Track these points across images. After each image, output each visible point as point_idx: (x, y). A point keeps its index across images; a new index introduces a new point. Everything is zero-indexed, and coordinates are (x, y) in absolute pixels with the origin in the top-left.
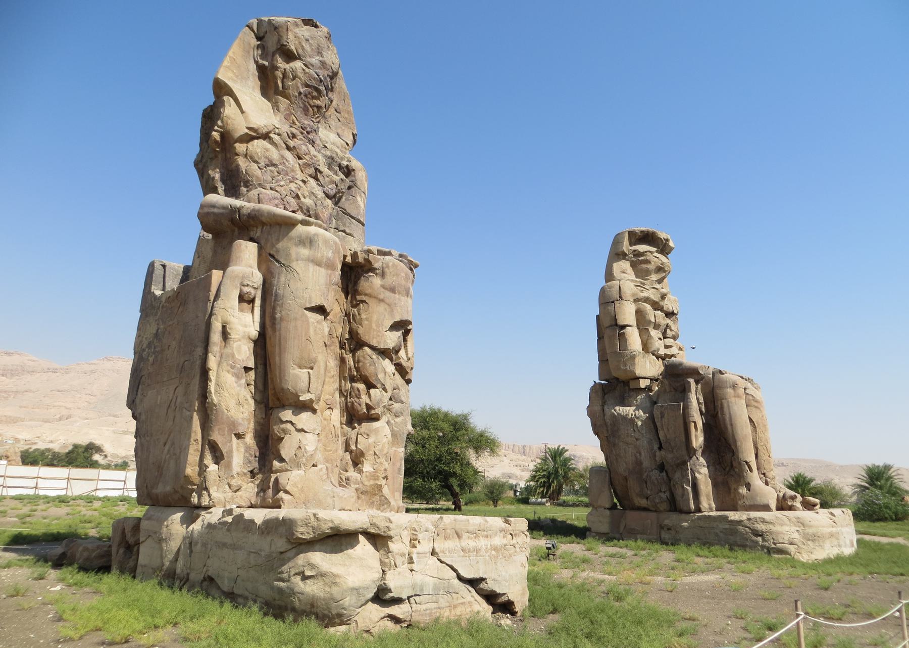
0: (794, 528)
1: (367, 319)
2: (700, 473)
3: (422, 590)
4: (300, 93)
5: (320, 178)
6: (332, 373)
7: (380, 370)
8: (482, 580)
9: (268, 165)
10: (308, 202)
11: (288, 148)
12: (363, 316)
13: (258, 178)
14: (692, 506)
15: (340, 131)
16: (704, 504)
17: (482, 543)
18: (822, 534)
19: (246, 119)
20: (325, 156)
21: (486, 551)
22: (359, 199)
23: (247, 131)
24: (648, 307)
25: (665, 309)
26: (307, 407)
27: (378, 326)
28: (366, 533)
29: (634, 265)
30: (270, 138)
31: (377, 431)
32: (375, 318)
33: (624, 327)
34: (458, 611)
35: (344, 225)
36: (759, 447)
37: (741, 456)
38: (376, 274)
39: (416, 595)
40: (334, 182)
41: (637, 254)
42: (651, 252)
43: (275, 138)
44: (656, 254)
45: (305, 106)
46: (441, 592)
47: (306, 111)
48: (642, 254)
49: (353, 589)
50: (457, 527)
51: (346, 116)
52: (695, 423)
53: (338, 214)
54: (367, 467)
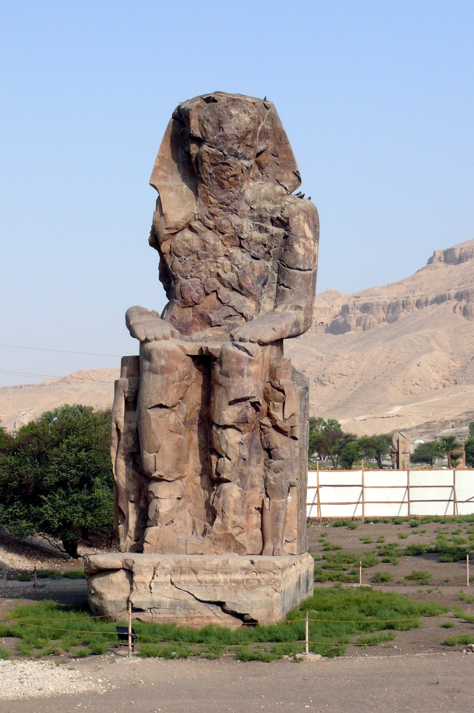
1: (213, 401)
4: (210, 174)
5: (245, 245)
7: (223, 442)
8: (224, 603)
9: (188, 255)
10: (228, 276)
11: (210, 229)
12: (212, 399)
13: (181, 272)
15: (278, 176)
19: (165, 219)
20: (252, 218)
21: (226, 582)
22: (296, 246)
23: (166, 232)
26: (160, 479)
28: (124, 569)
30: (191, 228)
31: (225, 492)
32: (217, 399)
34: (196, 621)
35: (284, 278)
38: (217, 362)
39: (154, 608)
43: (196, 224)
45: (219, 182)
46: (178, 607)
47: (221, 186)
49: (111, 601)
50: (193, 566)
51: (284, 156)
53: (279, 267)
54: (218, 521)
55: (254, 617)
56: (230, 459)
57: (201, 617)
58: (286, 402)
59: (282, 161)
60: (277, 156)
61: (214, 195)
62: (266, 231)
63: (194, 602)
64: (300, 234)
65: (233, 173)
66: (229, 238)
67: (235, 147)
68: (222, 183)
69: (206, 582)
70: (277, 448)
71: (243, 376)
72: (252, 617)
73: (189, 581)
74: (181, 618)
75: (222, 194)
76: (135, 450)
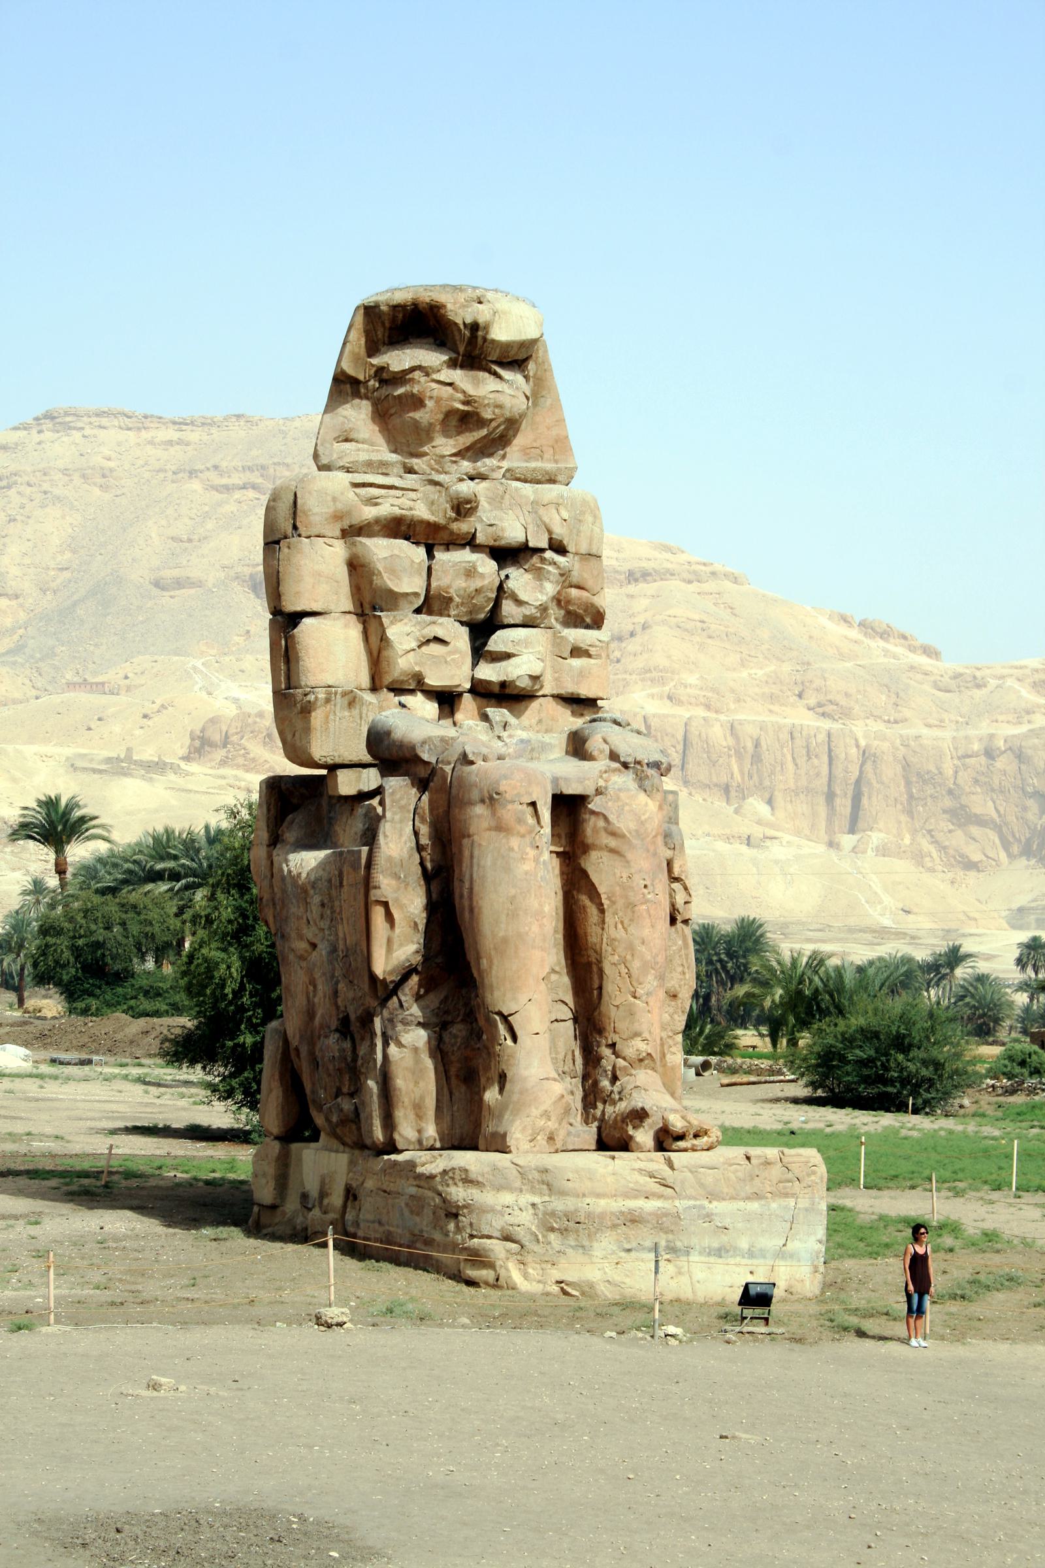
0: (527, 1198)
2: (400, 1045)
14: (379, 1134)
16: (406, 1131)
18: (589, 1215)
24: (382, 550)
25: (480, 539)
29: (382, 415)
33: (295, 618)
36: (608, 969)
37: (489, 999)
41: (387, 379)
42: (426, 371)
44: (447, 375)
48: (401, 378)
52: (386, 905)
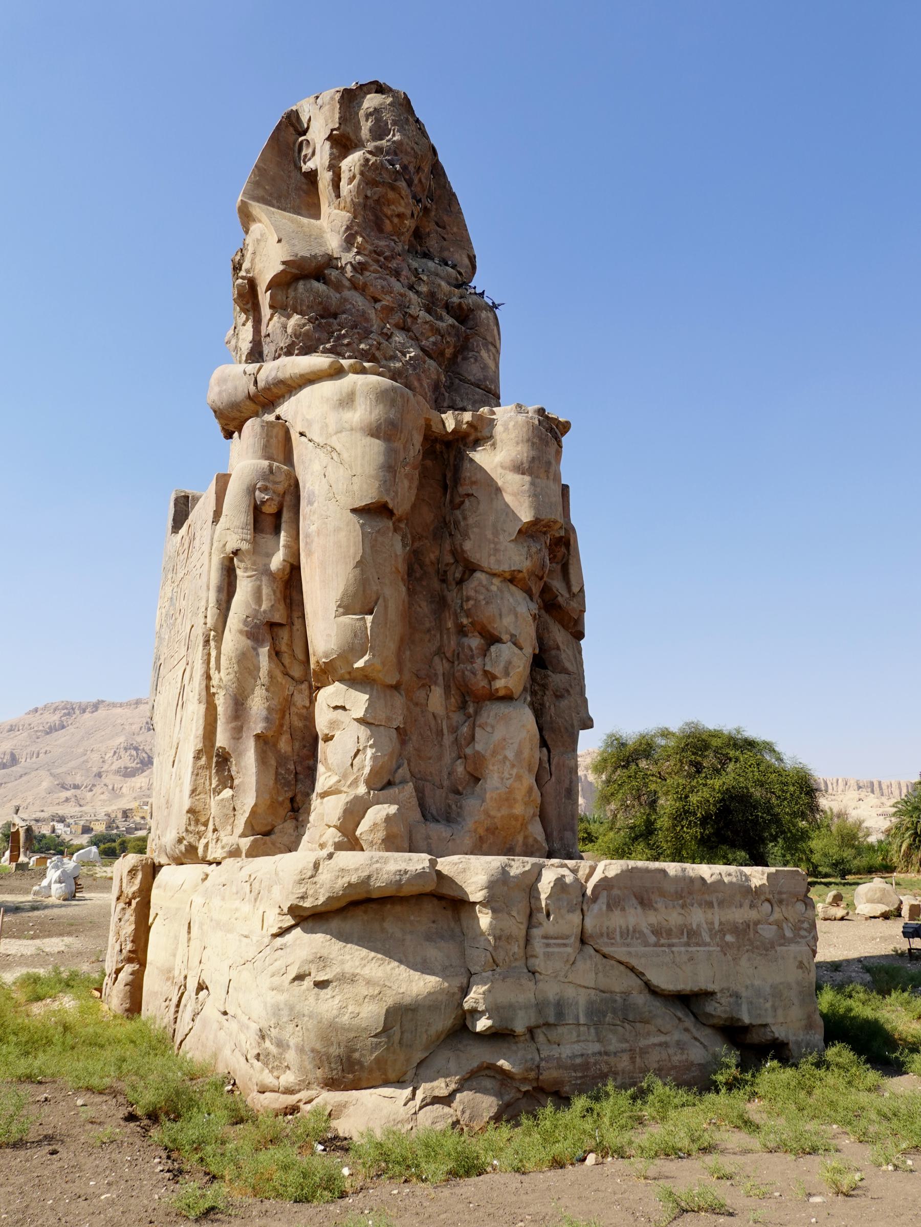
3: (560, 1014)
6: (428, 625)
7: (505, 610)
8: (708, 995)
9: (322, 317)
15: (446, 254)
17: (697, 917)
22: (484, 354)
23: (282, 267)
27: (496, 534)
40: (437, 331)
45: (377, 217)
46: (609, 1018)
51: (455, 230)
55: (779, 1032)
56: (521, 649)
57: (665, 1045)
58: (571, 562)
59: (450, 235)
60: (444, 228)
61: (368, 235)
62: (441, 319)
63: (641, 999)
64: (490, 339)
65: (401, 210)
66: (389, 310)
67: (411, 168)
68: (382, 220)
69: (669, 932)
70: (558, 648)
71: (548, 478)
72: (777, 1035)
73: (631, 929)
74: (615, 1054)
75: (379, 239)
76: (278, 618)
